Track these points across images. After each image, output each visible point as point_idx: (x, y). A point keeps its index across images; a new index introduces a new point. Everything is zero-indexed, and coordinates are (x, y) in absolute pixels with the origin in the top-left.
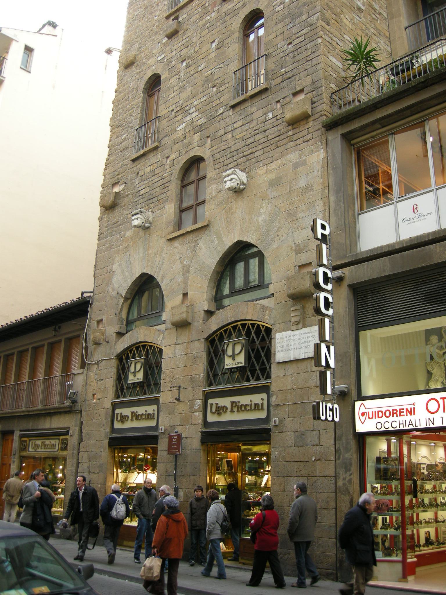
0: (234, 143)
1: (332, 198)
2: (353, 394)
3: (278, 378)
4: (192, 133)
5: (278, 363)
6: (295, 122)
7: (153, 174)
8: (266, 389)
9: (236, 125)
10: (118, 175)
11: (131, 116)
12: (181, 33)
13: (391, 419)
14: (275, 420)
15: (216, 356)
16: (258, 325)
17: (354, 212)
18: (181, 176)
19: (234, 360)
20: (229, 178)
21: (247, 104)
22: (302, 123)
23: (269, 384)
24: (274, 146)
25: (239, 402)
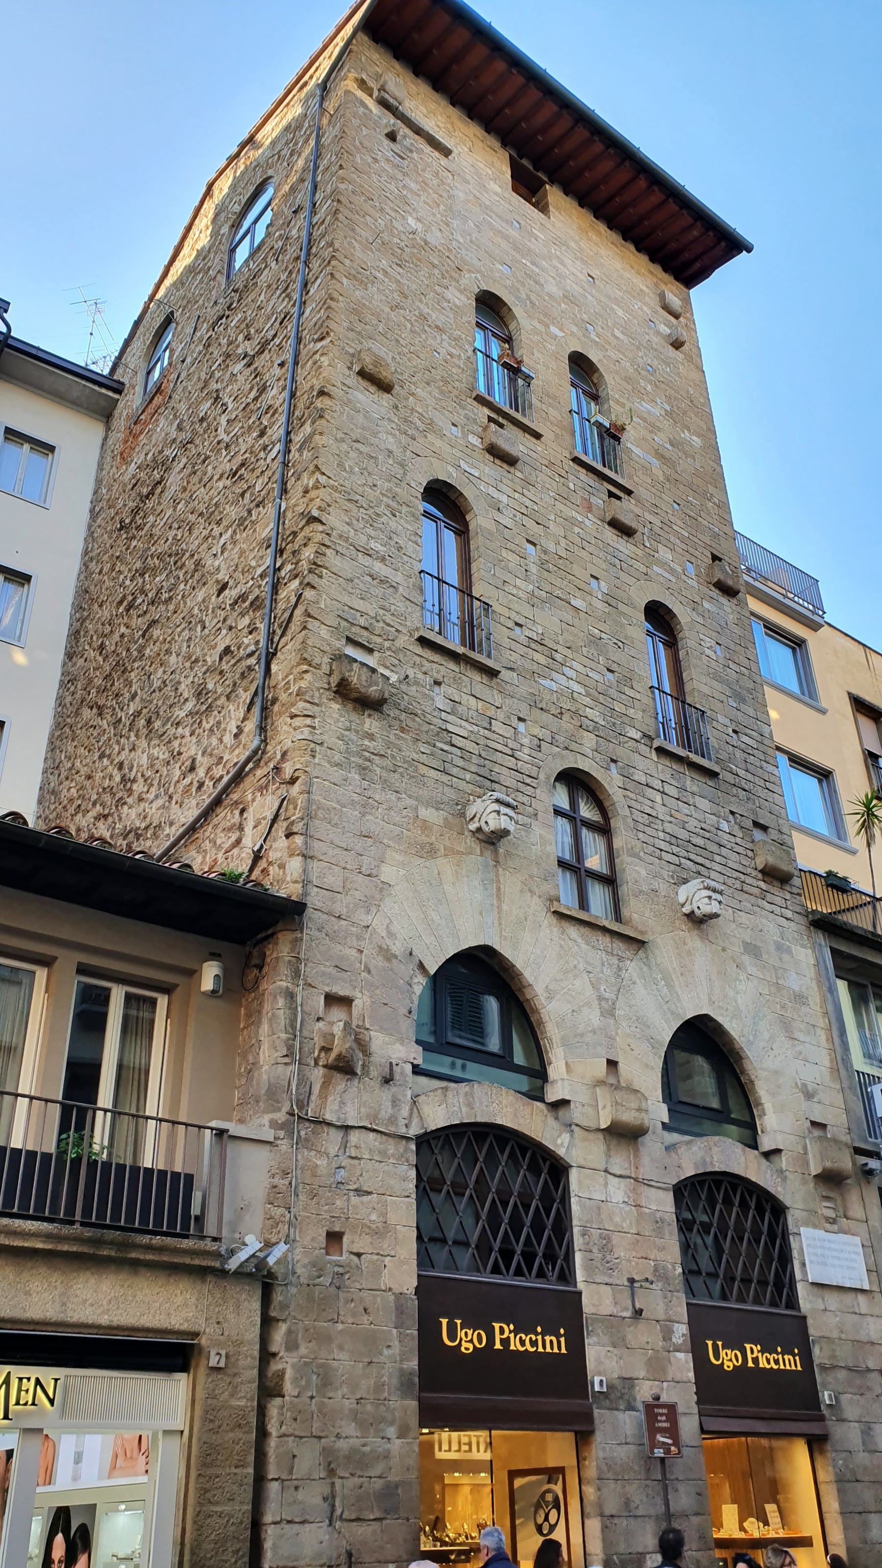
5: (812, 1283)
24: (738, 885)
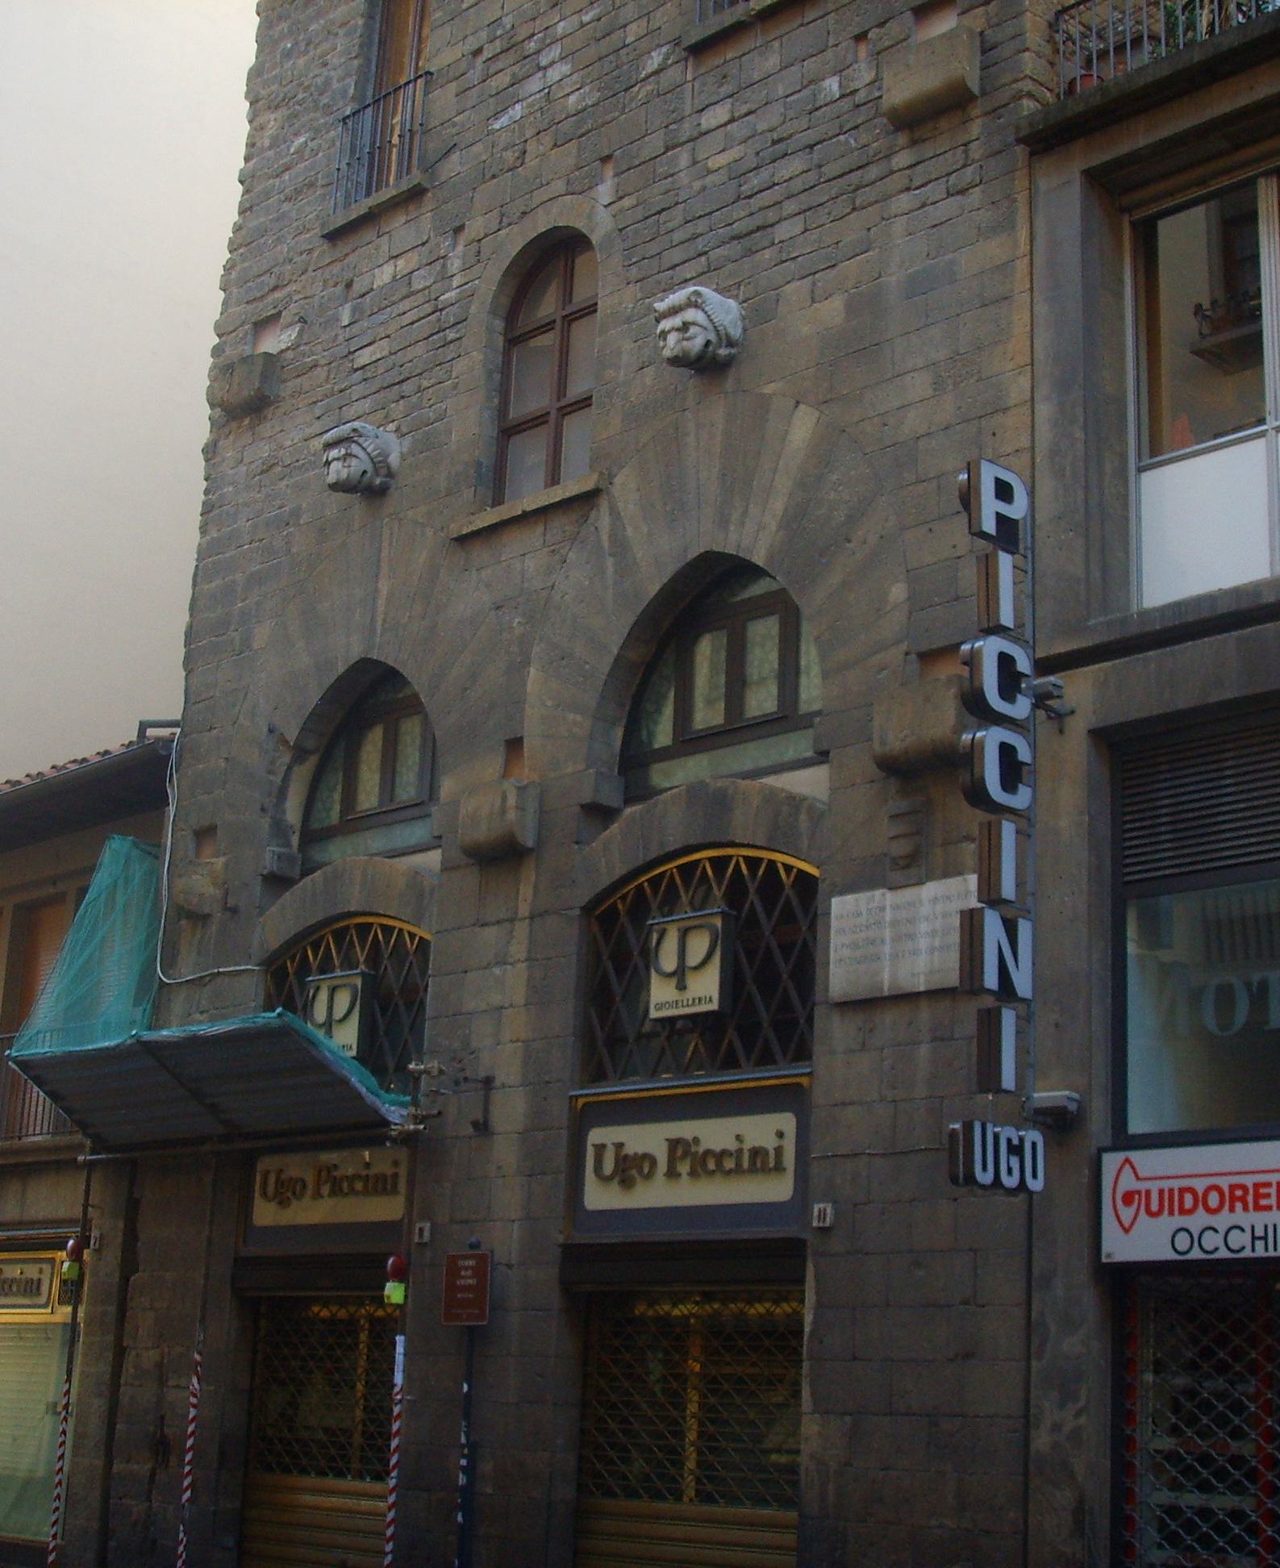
0: (697, 185)
1: (1044, 410)
2: (1098, 1122)
3: (840, 1059)
4: (547, 139)
6: (918, 121)
7: (404, 291)
8: (790, 1098)
9: (710, 119)
10: (275, 288)
11: (325, 65)
13: (1223, 1220)
14: (822, 1211)
15: (620, 971)
16: (772, 864)
17: (1123, 457)
18: (505, 301)
19: (682, 987)
20: (676, 321)
21: (750, 42)
22: (943, 124)
23: (804, 1081)
25: (696, 1140)
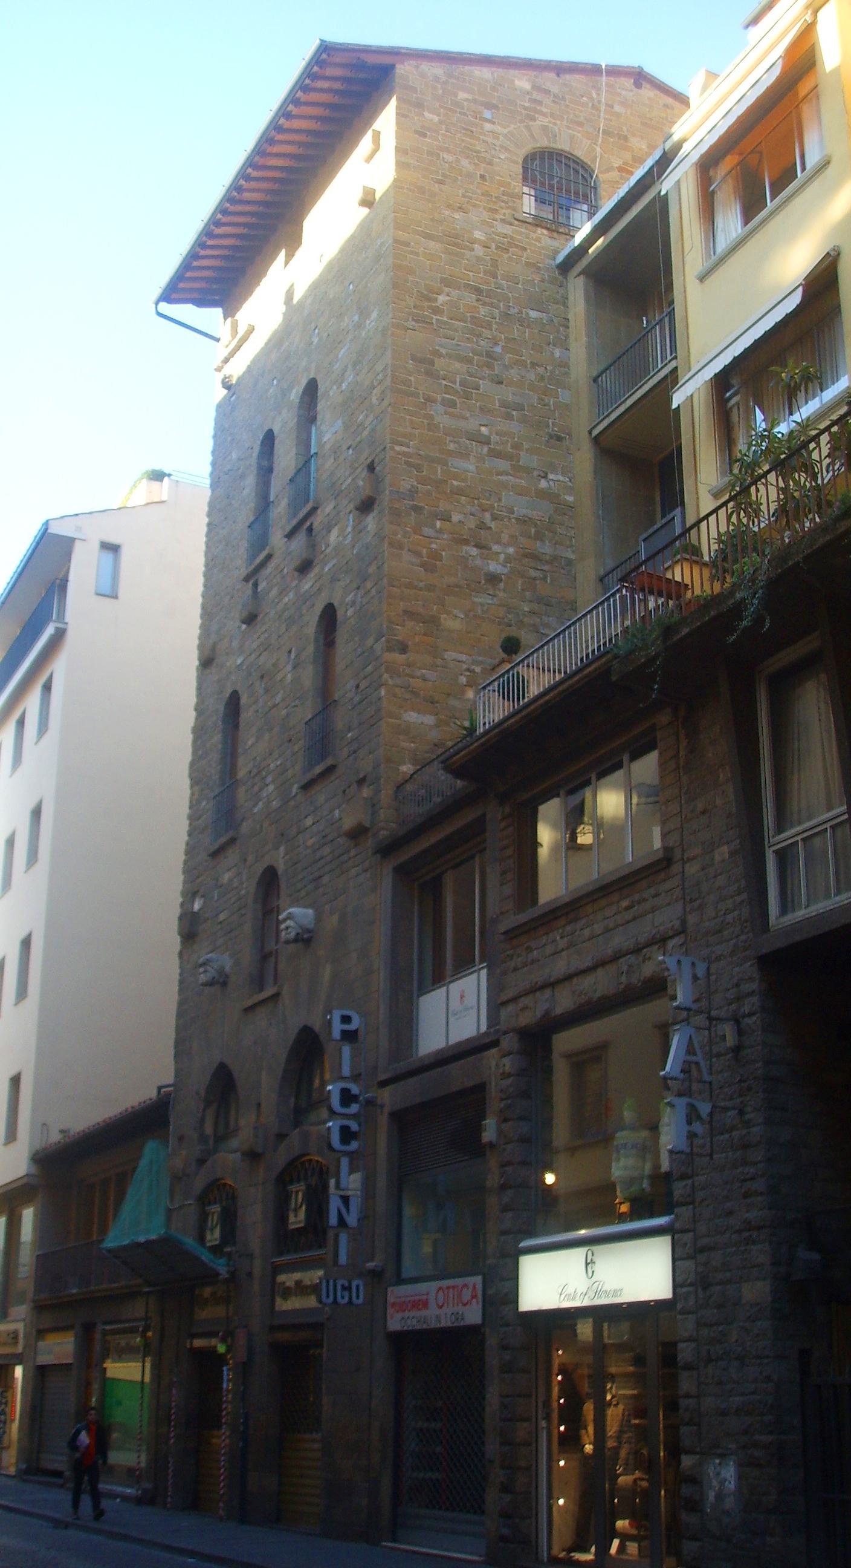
12: (259, 618)
